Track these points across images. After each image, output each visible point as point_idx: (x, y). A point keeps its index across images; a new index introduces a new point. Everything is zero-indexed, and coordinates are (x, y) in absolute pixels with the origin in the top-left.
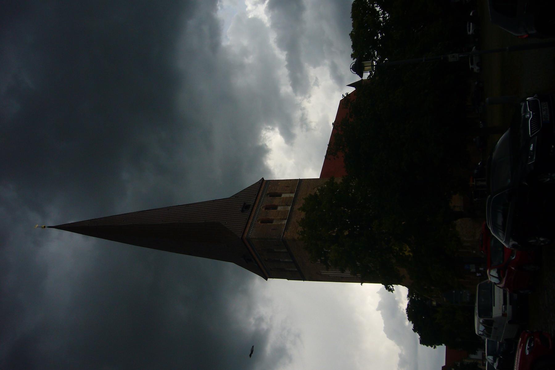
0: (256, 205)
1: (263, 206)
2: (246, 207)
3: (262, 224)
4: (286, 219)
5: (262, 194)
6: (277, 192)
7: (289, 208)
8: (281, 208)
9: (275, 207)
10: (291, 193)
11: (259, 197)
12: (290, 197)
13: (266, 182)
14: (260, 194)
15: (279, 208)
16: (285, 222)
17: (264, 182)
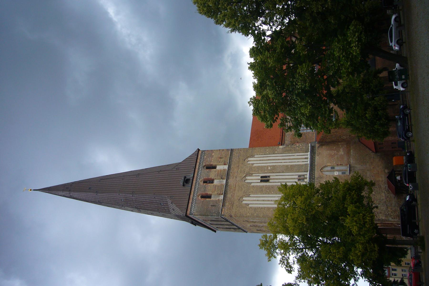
0: (195, 179)
1: (201, 180)
2: (186, 181)
3: (203, 199)
4: (222, 194)
6: (212, 164)
7: (225, 181)
8: (218, 182)
9: (212, 181)
10: (225, 164)
11: (197, 170)
13: (202, 153)
14: (197, 167)
15: (216, 182)
16: (222, 197)
17: (200, 152)
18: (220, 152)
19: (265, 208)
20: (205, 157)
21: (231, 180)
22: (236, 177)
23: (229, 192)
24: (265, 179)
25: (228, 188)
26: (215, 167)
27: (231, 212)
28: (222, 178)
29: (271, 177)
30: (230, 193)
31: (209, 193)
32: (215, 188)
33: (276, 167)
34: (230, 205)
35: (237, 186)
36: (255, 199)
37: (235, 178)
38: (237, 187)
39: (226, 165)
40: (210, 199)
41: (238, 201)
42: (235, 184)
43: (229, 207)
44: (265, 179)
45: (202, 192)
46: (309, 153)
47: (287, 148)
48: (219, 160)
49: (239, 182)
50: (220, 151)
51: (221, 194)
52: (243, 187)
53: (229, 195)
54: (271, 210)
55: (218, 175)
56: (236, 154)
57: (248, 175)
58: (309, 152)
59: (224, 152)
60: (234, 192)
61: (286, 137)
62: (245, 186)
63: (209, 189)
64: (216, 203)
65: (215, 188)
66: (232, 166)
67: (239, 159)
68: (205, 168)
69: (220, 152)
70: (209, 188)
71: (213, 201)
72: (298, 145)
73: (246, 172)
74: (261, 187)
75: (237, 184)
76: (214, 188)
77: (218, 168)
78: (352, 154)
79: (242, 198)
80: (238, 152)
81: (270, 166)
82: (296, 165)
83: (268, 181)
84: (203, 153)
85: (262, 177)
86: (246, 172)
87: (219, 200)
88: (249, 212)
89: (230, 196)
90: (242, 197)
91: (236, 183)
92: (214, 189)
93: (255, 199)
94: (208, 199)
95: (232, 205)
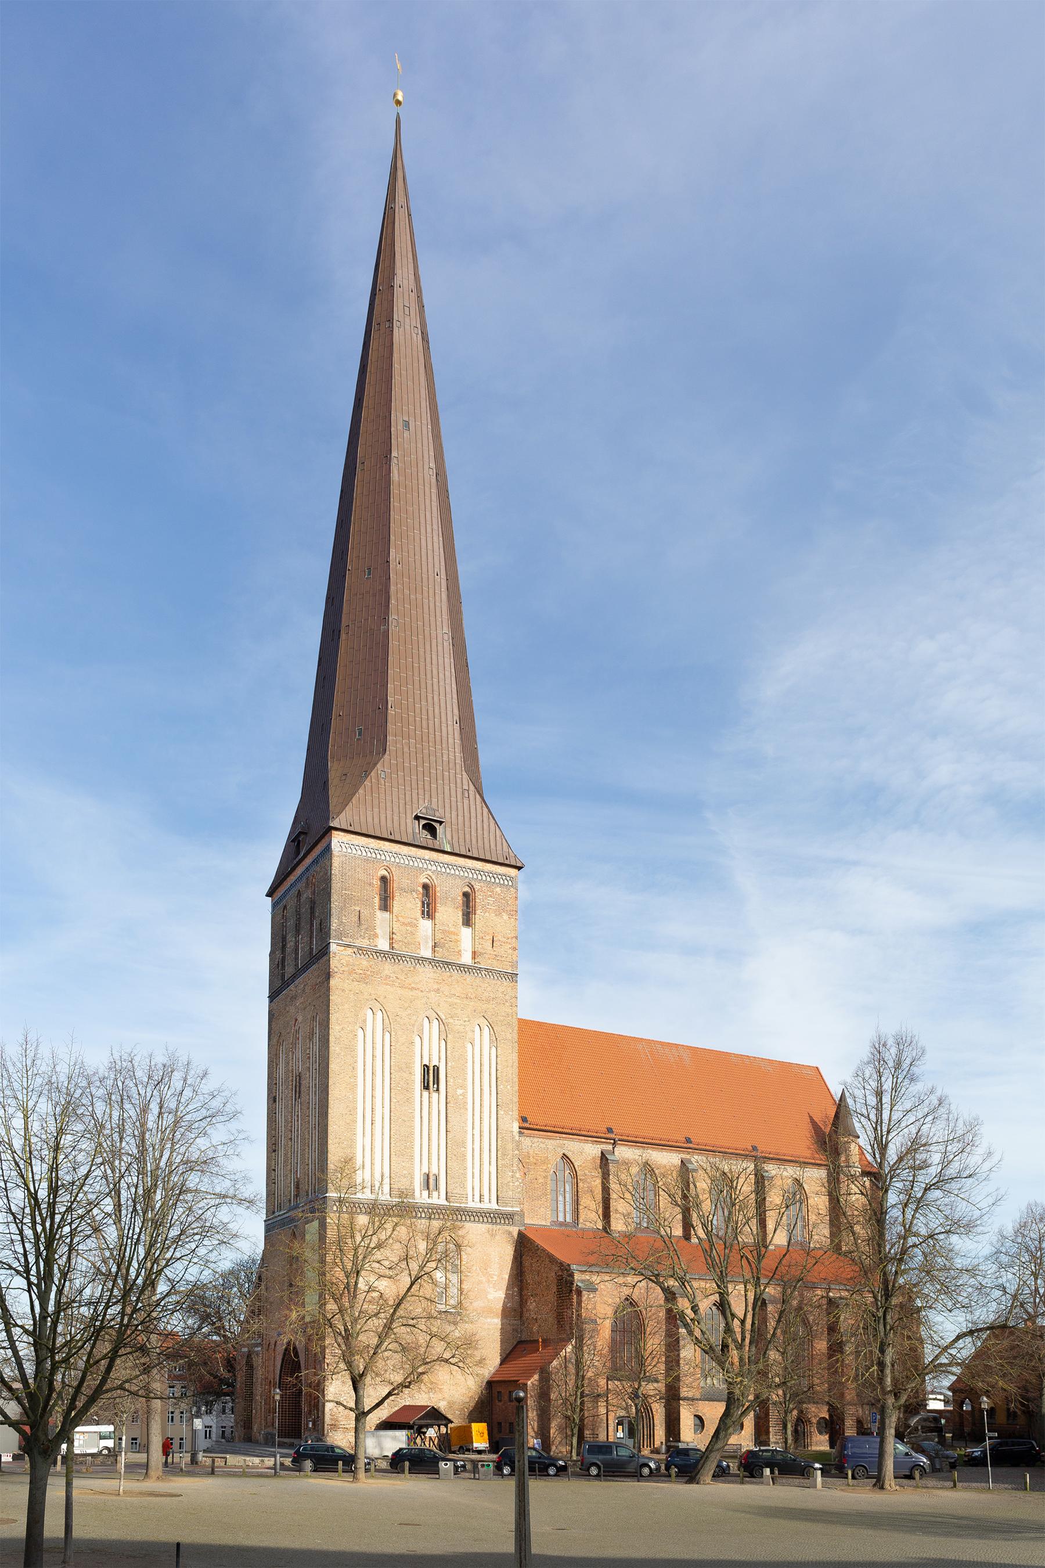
1: (433, 877)
3: (377, 883)
5: (289, 890)
6: (478, 912)
7: (427, 953)
9: (429, 911)
12: (459, 952)
15: (426, 925)
16: (383, 945)
17: (513, 872)
18: (509, 941)
19: (355, 1077)
20: (498, 889)
21: (432, 975)
22: (438, 991)
23: (396, 968)
24: (430, 1077)
25: (408, 966)
26: (467, 921)
27: (342, 976)
28: (435, 946)
29: (435, 1095)
30: (394, 972)
31: (397, 904)
32: (410, 924)
33: (462, 1111)
34: (361, 972)
35: (414, 993)
36: (379, 1046)
37: (436, 986)
38: (411, 993)
39: (474, 958)
40: (377, 907)
41: (374, 997)
42: (419, 986)
43: (355, 968)
44: (431, 1079)
45: (399, 881)
46: (494, 1206)
47: (510, 1146)
48: (488, 937)
49: (424, 1000)
50: (512, 938)
51: (391, 944)
52: (410, 1012)
53: (388, 968)
54: (348, 1094)
55: (444, 932)
56: (501, 989)
57: (442, 1026)
58: (497, 1208)
59: (510, 951)
60: (397, 984)
61: (540, 1140)
62: (414, 1018)
63: (408, 904)
64: (367, 929)
65: (410, 924)
66: (469, 978)
67: (488, 1001)
68: (467, 889)
69: (509, 941)
70: (409, 905)
71: (373, 915)
72: (518, 1175)
73: (451, 1021)
74: (409, 1067)
75: (420, 994)
76: (409, 920)
77: (466, 932)
78: (489, 1320)
79: (382, 1009)
80: (507, 997)
81: (464, 1095)
82: (465, 1169)
83: (424, 1086)
84: (510, 883)
85: (436, 1069)
86: (451, 1021)
87: (376, 936)
88: (342, 1029)
89: (386, 972)
90: (383, 1010)
91: (422, 991)
92: (407, 921)
93: (379, 1046)
94: (377, 900)
95: (364, 979)
